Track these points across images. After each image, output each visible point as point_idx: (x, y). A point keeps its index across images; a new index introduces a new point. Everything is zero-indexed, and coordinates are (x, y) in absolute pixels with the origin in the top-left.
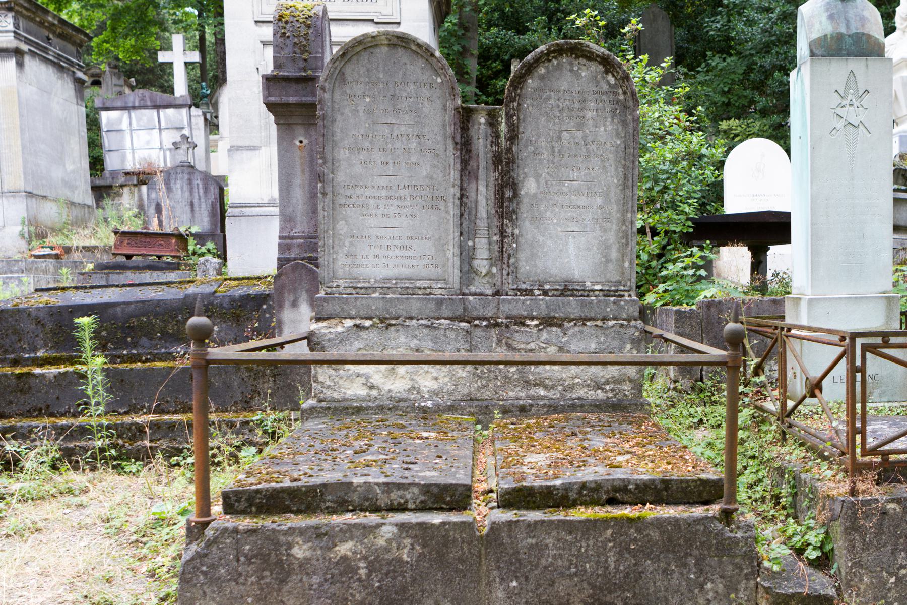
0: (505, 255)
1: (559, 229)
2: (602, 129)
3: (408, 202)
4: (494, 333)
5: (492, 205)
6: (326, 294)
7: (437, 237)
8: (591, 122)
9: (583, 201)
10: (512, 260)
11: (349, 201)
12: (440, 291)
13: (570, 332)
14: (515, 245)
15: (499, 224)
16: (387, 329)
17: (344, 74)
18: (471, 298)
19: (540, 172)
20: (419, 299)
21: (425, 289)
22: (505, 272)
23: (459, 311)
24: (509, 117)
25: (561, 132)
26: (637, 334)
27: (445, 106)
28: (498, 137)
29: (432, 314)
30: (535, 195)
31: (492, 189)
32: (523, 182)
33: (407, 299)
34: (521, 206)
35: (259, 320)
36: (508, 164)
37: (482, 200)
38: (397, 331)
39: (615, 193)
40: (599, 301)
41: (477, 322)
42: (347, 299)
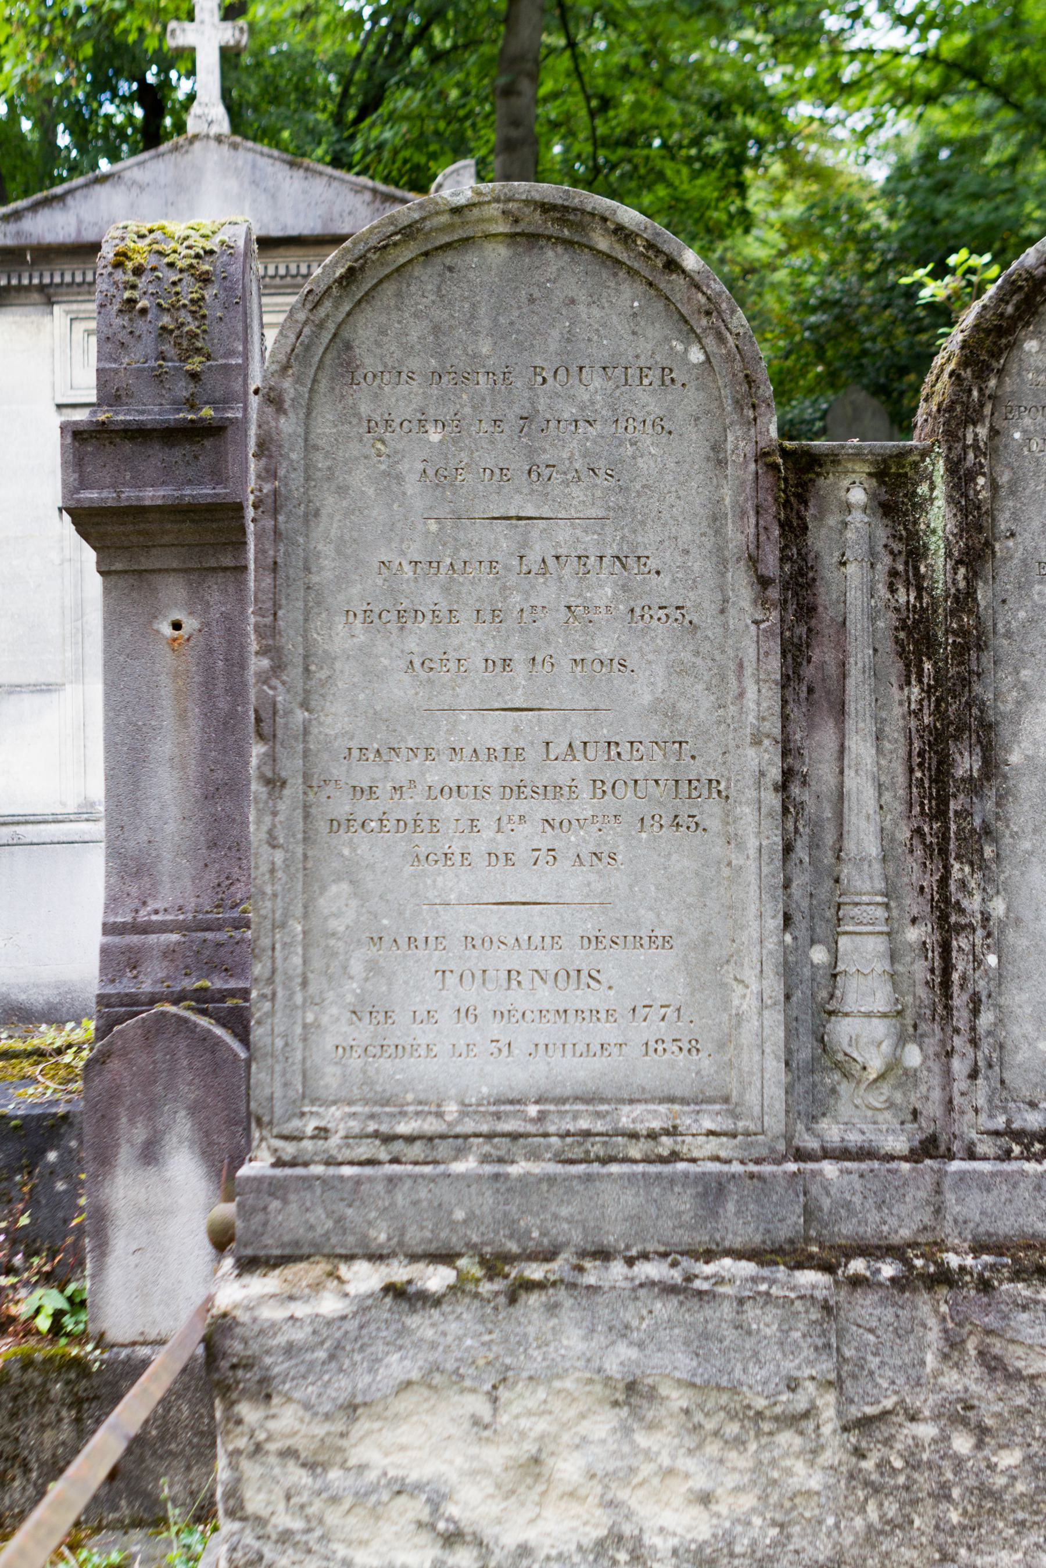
0: (960, 1000)
3: (585, 806)
4: (929, 1310)
5: (900, 808)
6: (279, 1163)
7: (695, 934)
10: (986, 1019)
11: (367, 808)
12: (712, 1146)
14: (992, 960)
15: (930, 881)
16: (513, 1300)
17: (348, 347)
18: (829, 1169)
20: (631, 1178)
21: (652, 1136)
22: (959, 1067)
23: (790, 1224)
24: (960, 478)
29: (684, 1238)
31: (896, 746)
32: (1015, 718)
33: (588, 1178)
34: (1011, 808)
35: (32, 1203)
36: (961, 651)
37: (860, 788)
38: (552, 1308)
41: (858, 1266)
42: (358, 1181)
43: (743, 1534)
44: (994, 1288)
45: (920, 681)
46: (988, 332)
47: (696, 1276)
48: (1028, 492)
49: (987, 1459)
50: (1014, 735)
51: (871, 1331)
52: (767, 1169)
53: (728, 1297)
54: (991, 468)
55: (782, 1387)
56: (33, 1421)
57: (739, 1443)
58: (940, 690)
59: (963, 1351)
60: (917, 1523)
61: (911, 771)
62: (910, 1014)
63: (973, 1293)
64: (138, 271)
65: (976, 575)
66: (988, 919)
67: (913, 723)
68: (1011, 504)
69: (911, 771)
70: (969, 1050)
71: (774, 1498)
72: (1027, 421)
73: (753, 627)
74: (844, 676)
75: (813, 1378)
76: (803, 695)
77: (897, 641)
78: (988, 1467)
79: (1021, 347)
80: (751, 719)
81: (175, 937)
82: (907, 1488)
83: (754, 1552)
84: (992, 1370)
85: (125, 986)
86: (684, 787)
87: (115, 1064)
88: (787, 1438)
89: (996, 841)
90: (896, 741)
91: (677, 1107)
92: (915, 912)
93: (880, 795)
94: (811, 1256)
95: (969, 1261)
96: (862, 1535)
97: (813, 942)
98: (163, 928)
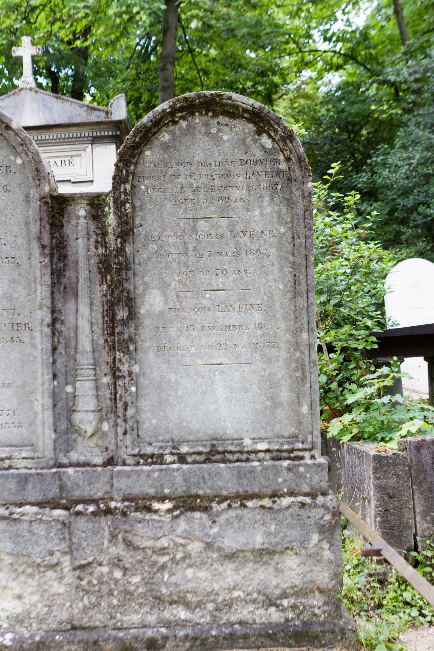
0: (120, 405)
1: (200, 362)
2: (257, 212)
4: (105, 523)
5: (100, 332)
7: (20, 382)
8: (239, 204)
9: (233, 318)
10: (130, 412)
12: (25, 463)
13: (222, 519)
14: (133, 389)
15: (110, 360)
18: (70, 471)
19: (167, 280)
23: (53, 491)
25: (196, 220)
26: (328, 517)
27: (27, 196)
28: (104, 234)
29: (13, 498)
30: (161, 315)
31: (98, 308)
32: (142, 296)
34: (141, 330)
36: (119, 271)
37: (84, 325)
39: (281, 303)
40: (265, 468)
41: (80, 507)
43: (34, 610)
44: (128, 515)
45: (106, 283)
46: (129, 148)
47: (14, 513)
48: (147, 209)
49: (127, 580)
50: (142, 302)
51: (84, 532)
52: (44, 471)
53: (24, 520)
54: (132, 200)
55: (47, 554)
57: (32, 575)
58: (112, 287)
59: (117, 539)
60: (102, 605)
61: (104, 317)
62: (104, 411)
63: (120, 517)
65: (125, 241)
66: (131, 373)
67: (104, 299)
68: (140, 214)
69: (104, 317)
70: (123, 424)
71: (46, 597)
72: (146, 182)
73: (39, 264)
74: (78, 281)
75: (59, 551)
76: (62, 289)
77: (99, 268)
78: (128, 582)
79: (144, 154)
80: (39, 299)
82: (99, 591)
83: (38, 617)
84: (128, 546)
86: (15, 326)
88: (50, 574)
89: (135, 343)
90: (98, 306)
91: (13, 448)
92: (105, 372)
93: (92, 327)
94: (59, 504)
95: (119, 505)
96: (82, 609)
97: (67, 384)
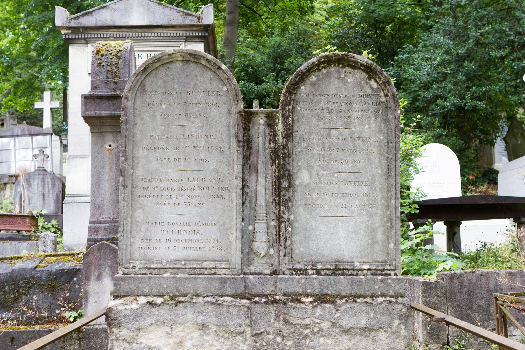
0: (282, 238)
1: (330, 215)
2: (367, 126)
3: (197, 192)
4: (272, 309)
5: (271, 194)
6: (124, 274)
7: (221, 222)
8: (356, 121)
9: (351, 189)
10: (288, 243)
11: (146, 193)
12: (224, 271)
13: (342, 309)
14: (290, 229)
15: (276, 211)
16: (176, 305)
17: (144, 86)
18: (251, 277)
19: (312, 164)
20: (205, 278)
21: (210, 269)
22: (282, 254)
23: (241, 289)
24: (285, 118)
25: (330, 129)
26: (404, 310)
27: (229, 110)
28: (275, 135)
29: (217, 292)
30: (308, 185)
31: (270, 180)
32: (297, 174)
33: (195, 278)
34: (295, 194)
35: (70, 290)
36: (284, 158)
38: (185, 307)
39: (379, 182)
40: (368, 280)
41: (257, 299)
42: (142, 278)
46: (292, 85)
51: (259, 314)
52: (236, 276)
53: (225, 305)
56: (68, 343)
57: (228, 339)
59: (279, 318)
61: (273, 185)
62: (271, 242)
64: (102, 55)
65: (288, 140)
67: (274, 175)
69: (273, 185)
70: (284, 250)
72: (301, 105)
76: (248, 168)
77: (270, 155)
80: (235, 173)
81: (107, 225)
85: (94, 237)
86: (220, 189)
87: (91, 256)
88: (239, 338)
89: (292, 202)
94: (245, 296)
95: (281, 298)
97: (249, 225)
98: (105, 222)
